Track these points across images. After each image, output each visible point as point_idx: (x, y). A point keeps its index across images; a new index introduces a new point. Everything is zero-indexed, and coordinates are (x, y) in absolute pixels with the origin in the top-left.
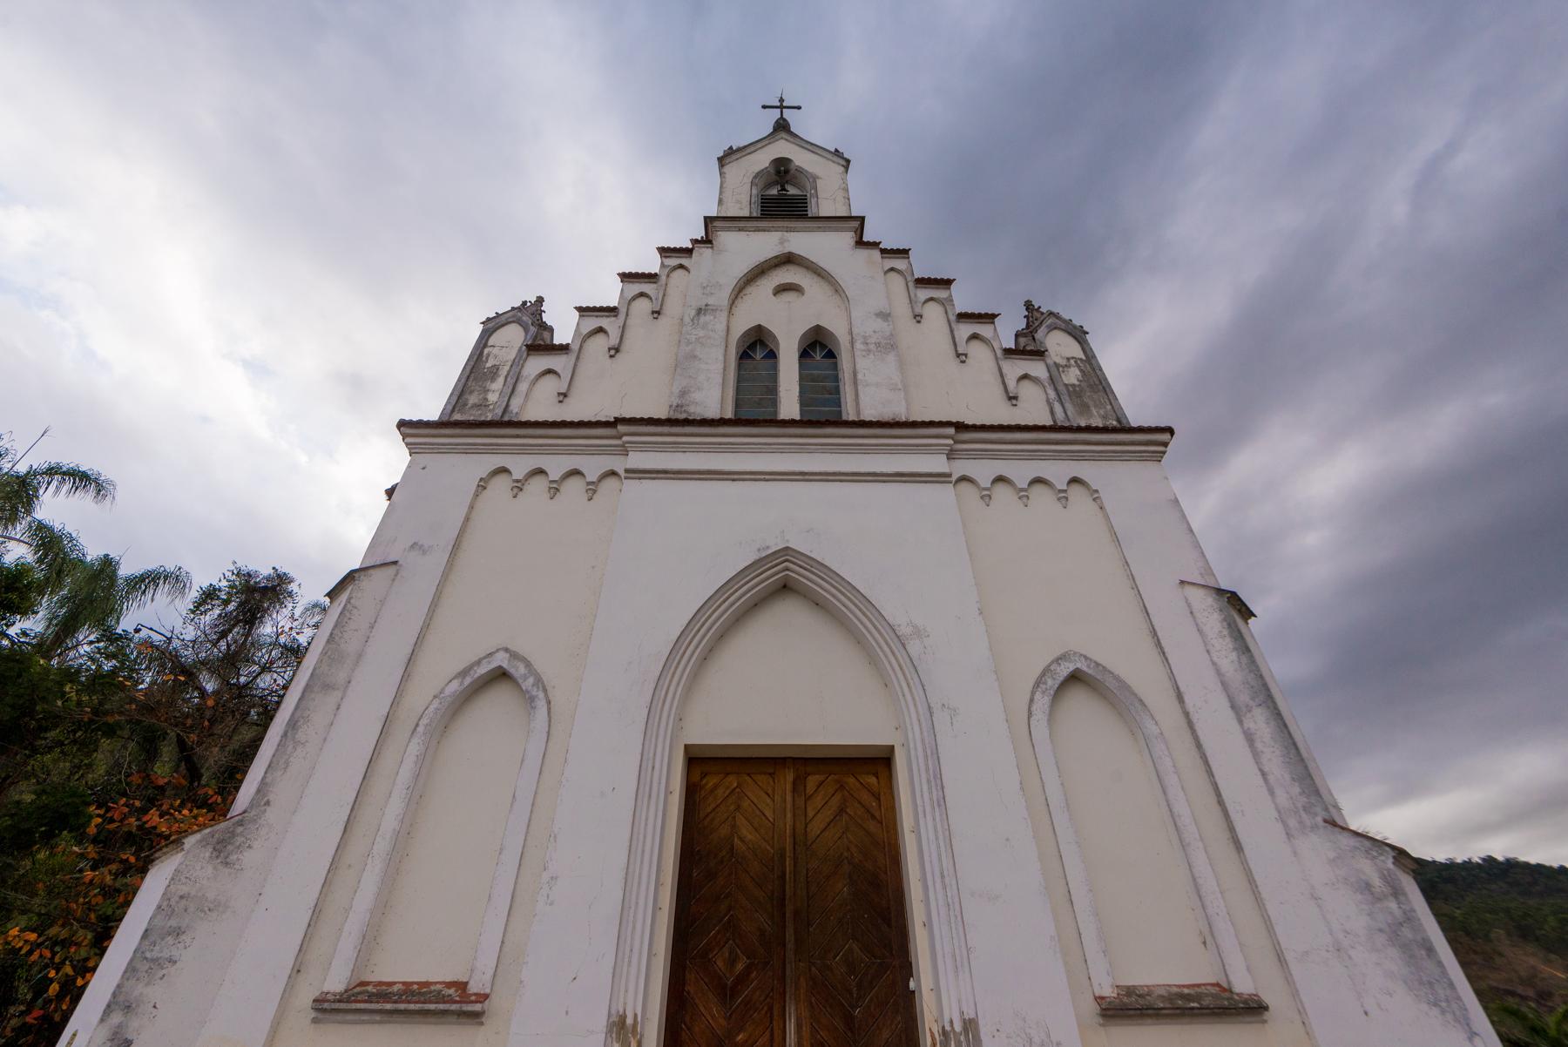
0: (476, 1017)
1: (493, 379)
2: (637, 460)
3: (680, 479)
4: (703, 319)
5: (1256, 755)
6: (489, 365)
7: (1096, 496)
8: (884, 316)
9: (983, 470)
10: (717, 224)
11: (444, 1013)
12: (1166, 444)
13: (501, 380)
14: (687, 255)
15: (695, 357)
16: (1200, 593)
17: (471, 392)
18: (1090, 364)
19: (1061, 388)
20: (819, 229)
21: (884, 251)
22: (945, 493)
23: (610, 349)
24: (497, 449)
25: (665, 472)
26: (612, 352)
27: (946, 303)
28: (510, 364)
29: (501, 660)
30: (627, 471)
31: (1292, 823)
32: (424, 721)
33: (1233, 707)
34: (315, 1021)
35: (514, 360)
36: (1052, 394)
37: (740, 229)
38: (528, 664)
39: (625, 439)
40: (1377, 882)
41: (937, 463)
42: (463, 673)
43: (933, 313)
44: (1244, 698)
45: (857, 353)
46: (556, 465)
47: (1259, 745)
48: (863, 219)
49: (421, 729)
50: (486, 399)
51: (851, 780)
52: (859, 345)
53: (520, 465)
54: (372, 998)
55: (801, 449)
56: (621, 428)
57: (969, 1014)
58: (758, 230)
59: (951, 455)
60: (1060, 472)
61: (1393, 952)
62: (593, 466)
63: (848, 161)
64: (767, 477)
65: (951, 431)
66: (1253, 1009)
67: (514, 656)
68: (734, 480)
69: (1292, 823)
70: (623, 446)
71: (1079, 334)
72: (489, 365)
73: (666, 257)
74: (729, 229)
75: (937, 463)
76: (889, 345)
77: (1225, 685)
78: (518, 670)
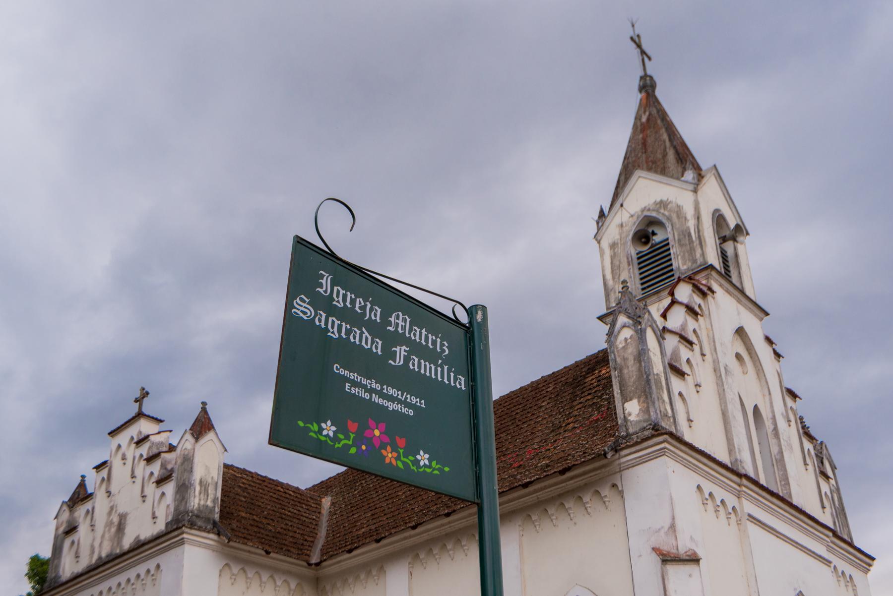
1: (663, 392)
2: (749, 507)
3: (820, 561)
6: (655, 373)
7: (854, 588)
12: (870, 565)
14: (701, 296)
18: (838, 489)
19: (837, 509)
24: (697, 470)
25: (759, 521)
28: (663, 375)
30: (750, 515)
35: (665, 373)
36: (834, 514)
39: (744, 489)
41: (821, 550)
45: (783, 447)
50: (666, 410)
52: (782, 441)
53: (708, 487)
55: (791, 523)
56: (745, 481)
60: (849, 570)
62: (731, 501)
64: (787, 540)
65: (831, 534)
68: (777, 537)
70: (739, 491)
71: (834, 468)
72: (655, 373)
73: (694, 292)
74: (716, 281)
75: (821, 550)
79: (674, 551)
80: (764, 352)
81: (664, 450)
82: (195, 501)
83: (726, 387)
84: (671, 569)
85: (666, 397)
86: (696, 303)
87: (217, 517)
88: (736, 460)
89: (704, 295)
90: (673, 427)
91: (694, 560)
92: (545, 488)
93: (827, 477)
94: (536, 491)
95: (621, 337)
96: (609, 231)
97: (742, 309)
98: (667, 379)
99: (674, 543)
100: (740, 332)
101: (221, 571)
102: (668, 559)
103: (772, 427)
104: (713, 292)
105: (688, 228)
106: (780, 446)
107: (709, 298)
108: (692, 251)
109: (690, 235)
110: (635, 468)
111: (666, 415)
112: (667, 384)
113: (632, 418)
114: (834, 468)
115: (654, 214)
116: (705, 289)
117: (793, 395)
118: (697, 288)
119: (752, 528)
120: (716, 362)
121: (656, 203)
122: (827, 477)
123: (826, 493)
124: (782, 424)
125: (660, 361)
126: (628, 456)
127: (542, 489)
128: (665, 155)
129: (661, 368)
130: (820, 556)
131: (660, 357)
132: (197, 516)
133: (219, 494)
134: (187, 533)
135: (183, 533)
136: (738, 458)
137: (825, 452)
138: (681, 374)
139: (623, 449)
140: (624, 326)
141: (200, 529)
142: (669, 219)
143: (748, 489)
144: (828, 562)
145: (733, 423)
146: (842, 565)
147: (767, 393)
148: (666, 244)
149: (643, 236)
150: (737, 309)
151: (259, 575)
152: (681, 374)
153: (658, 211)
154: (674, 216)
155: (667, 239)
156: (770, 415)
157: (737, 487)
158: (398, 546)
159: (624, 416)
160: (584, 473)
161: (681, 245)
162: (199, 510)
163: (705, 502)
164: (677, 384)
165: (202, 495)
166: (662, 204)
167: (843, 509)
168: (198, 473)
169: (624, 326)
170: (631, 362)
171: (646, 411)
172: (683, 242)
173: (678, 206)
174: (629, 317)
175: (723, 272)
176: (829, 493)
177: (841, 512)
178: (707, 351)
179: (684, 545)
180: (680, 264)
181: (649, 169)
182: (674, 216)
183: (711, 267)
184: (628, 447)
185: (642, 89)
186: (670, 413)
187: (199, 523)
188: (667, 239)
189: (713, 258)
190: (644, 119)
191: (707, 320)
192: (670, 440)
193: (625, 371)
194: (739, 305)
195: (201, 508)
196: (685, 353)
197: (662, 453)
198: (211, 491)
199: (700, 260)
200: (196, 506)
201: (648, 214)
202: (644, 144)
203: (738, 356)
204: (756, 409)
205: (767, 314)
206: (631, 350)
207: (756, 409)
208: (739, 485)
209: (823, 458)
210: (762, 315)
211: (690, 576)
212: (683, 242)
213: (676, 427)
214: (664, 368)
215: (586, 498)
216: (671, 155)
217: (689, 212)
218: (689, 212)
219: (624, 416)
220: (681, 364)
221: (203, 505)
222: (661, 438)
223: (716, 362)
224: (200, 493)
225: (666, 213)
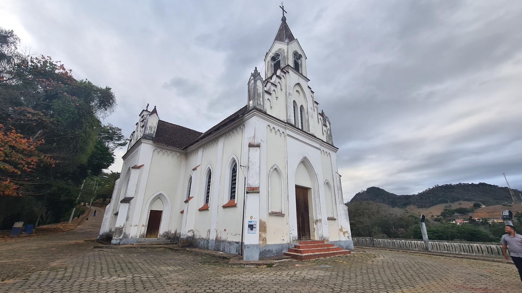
0: (283, 216)
1: (260, 98)
2: (288, 132)
4: (290, 97)
5: (338, 195)
6: (258, 92)
8: (312, 109)
9: (322, 148)
10: (289, 67)
11: (280, 216)
13: (262, 98)
15: (290, 107)
16: (338, 175)
17: (258, 100)
18: (330, 129)
20: (303, 78)
21: (311, 91)
22: (319, 152)
23: (276, 97)
26: (277, 98)
27: (317, 108)
28: (262, 93)
29: (276, 167)
30: (288, 134)
31: (340, 203)
32: (270, 175)
33: (338, 189)
34: (269, 216)
35: (263, 93)
37: (292, 71)
38: (279, 168)
39: (287, 127)
40: (346, 210)
42: (272, 168)
43: (315, 109)
44: (339, 189)
46: (277, 128)
47: (339, 194)
48: (310, 80)
49: (270, 176)
51: (304, 191)
52: (309, 115)
53: (272, 126)
54: (275, 214)
55: (306, 137)
56: (287, 124)
57: (321, 219)
58: (295, 73)
59: (320, 145)
60: (328, 151)
61: (345, 216)
62: (282, 130)
63: (307, 58)
65: (321, 141)
66: (335, 219)
67: (277, 166)
69: (340, 203)
74: (291, 70)
75: (318, 146)
76: (312, 117)
77: (337, 187)
78: (278, 169)
79: (253, 144)
80: (307, 92)
81: (254, 113)
82: (147, 132)
83: (288, 98)
84: (251, 149)
85: (261, 99)
86: (282, 75)
87: (154, 136)
88: (288, 119)
89: (285, 73)
90: (262, 108)
91: (258, 146)
92: (230, 127)
93: (326, 126)
94: (227, 128)
95: (251, 83)
96: (268, 58)
97: (300, 78)
98: (263, 94)
99: (254, 141)
100: (298, 84)
101: (154, 151)
102: (251, 146)
103: (307, 111)
104: (289, 73)
105: (285, 55)
106: (308, 116)
107: (287, 74)
108: (285, 61)
109: (285, 57)
110: (248, 120)
111: (260, 105)
112: (263, 96)
113: (250, 106)
114: (330, 124)
115: (278, 52)
116: (285, 71)
117: (317, 104)
118: (282, 71)
119: (288, 138)
120: (286, 91)
121: (278, 49)
122: (326, 126)
123: (325, 130)
124: (310, 110)
125: (262, 89)
126: (247, 116)
127: (229, 127)
128: (283, 37)
129: (262, 91)
130: (316, 147)
131: (262, 88)
132: (147, 136)
133: (156, 130)
134: (142, 140)
135: (141, 140)
136: (289, 118)
137: (327, 119)
138: (270, 94)
139: (245, 114)
140: (252, 80)
141: (148, 139)
142: (281, 53)
143: (288, 127)
144: (320, 149)
145: (288, 108)
146: (326, 150)
147: (306, 102)
148: (280, 61)
149: (273, 59)
150: (298, 78)
151: (162, 151)
152: (270, 94)
153: (279, 51)
154: (282, 52)
155: (280, 60)
156: (307, 108)
157: (285, 126)
158: (203, 143)
159: (249, 105)
160: (238, 122)
161: (283, 60)
162: (148, 134)
163: (271, 130)
164: (267, 96)
165: (150, 130)
166: (280, 49)
167: (331, 135)
168: (149, 125)
169: (252, 80)
170: (252, 90)
171: (253, 103)
172: (283, 59)
173: (283, 49)
174: (253, 77)
175: (294, 67)
176: (326, 130)
177: (330, 136)
178: (283, 88)
179: (256, 142)
180: (282, 66)
181: (280, 41)
182: (282, 52)
183: (288, 65)
184: (246, 114)
185: (282, 20)
186: (262, 104)
187: (148, 138)
188: (280, 60)
189: (291, 63)
190: (281, 28)
191: (285, 80)
192: (256, 111)
193: (251, 92)
194: (299, 77)
195: (149, 134)
196: (273, 88)
197: (254, 115)
198: (153, 129)
199: (287, 64)
200: (147, 133)
201: (276, 52)
202: (280, 35)
203: (297, 91)
204: (302, 107)
205: (310, 80)
206: (253, 86)
207: (302, 107)
208: (286, 126)
209: (326, 121)
210: (308, 80)
211: (256, 151)
212: (283, 59)
213: (263, 108)
214: (263, 91)
215: (238, 129)
216: (285, 36)
217: (286, 51)
218: (286, 51)
219: (249, 105)
220: (270, 91)
221: (150, 133)
222: (253, 111)
223: (286, 91)
224: (149, 130)
225: (281, 52)
